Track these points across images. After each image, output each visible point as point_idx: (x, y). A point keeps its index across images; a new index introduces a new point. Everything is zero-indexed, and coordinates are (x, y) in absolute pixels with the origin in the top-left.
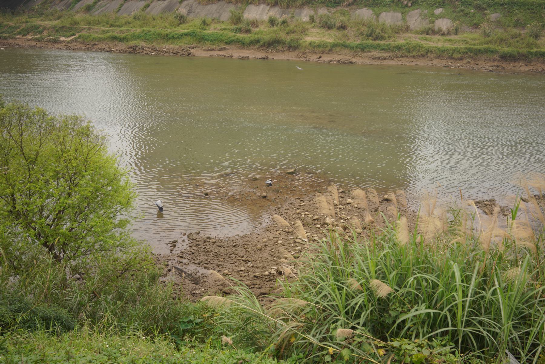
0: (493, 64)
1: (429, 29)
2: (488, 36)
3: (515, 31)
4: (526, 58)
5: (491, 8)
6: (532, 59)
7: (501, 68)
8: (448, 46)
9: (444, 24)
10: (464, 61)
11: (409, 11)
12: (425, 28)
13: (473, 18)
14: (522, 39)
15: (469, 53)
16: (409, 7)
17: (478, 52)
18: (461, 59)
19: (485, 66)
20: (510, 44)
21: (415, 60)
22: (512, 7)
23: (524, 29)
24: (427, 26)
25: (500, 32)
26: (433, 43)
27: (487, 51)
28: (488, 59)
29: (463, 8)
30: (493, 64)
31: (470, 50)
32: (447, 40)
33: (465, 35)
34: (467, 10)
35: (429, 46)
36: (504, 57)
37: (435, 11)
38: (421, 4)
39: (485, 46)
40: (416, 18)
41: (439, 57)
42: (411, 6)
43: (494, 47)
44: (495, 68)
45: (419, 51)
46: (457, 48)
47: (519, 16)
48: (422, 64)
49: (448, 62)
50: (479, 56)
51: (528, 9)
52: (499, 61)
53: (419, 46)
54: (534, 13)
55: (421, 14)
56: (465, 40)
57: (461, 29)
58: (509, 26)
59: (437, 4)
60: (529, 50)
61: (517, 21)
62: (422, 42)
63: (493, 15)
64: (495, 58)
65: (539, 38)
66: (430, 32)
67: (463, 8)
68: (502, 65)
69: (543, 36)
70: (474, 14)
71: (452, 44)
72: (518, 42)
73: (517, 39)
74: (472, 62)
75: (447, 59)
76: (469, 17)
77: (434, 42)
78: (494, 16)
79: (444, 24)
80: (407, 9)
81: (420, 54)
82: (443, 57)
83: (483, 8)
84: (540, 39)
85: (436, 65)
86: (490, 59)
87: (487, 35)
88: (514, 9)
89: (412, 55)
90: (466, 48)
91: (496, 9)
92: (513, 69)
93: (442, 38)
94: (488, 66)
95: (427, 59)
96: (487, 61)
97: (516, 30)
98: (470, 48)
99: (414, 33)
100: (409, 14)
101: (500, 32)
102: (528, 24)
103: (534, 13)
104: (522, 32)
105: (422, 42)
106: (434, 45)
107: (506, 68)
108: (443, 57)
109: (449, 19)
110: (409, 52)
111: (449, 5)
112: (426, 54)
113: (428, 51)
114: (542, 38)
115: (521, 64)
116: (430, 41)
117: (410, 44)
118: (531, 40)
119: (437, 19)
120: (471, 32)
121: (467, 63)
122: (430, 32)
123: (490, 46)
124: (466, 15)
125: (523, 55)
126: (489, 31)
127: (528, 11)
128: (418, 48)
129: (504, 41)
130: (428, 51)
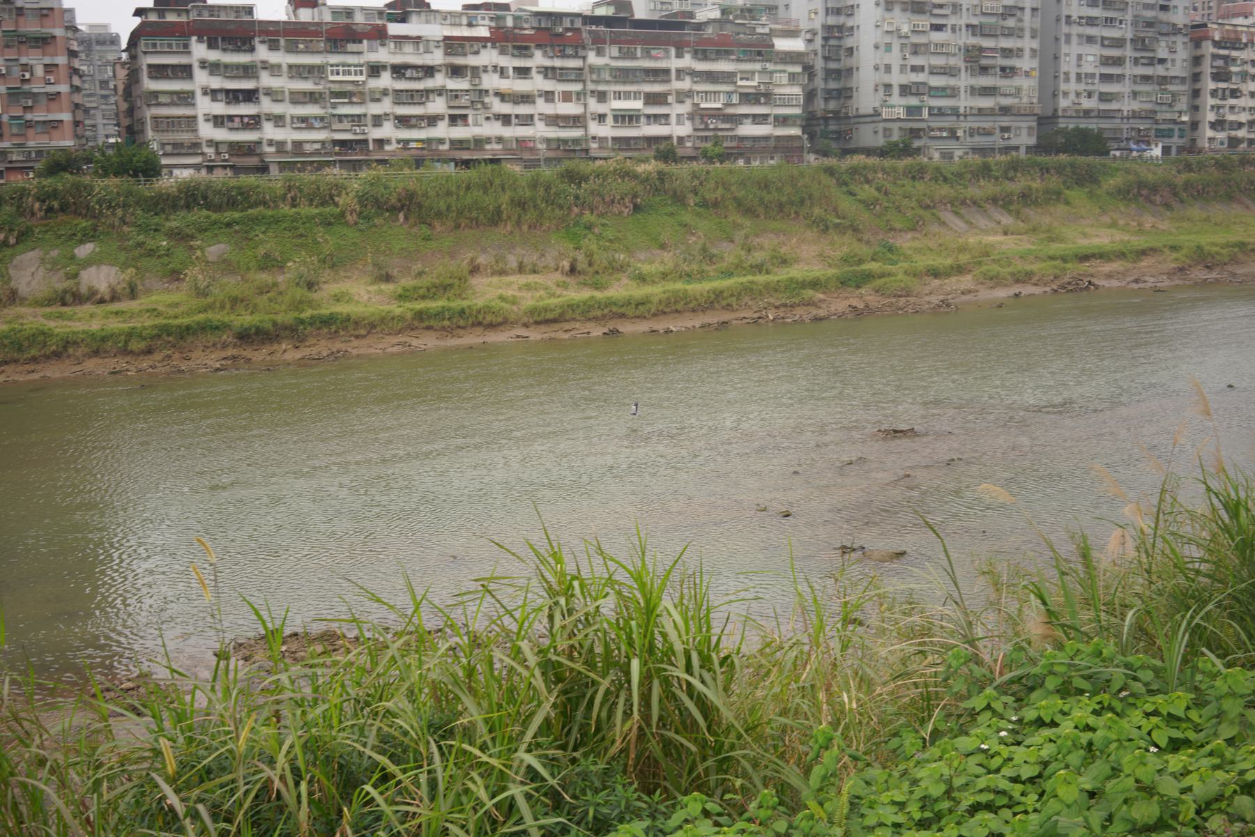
0: (224, 354)
1: (65, 292)
2: (202, 293)
3: (265, 277)
4: (294, 332)
5: (206, 234)
6: (306, 332)
7: (242, 361)
8: (115, 325)
9: (101, 278)
10: (158, 356)
11: (13, 256)
12: (56, 291)
13: (166, 260)
14: (281, 293)
15: (164, 335)
16: (13, 246)
17: (185, 332)
18: (149, 351)
19: (205, 359)
20: (255, 306)
21: (39, 367)
22: (252, 228)
23: (284, 273)
24: (60, 286)
25: (231, 285)
26: (78, 324)
27: (204, 328)
28: (210, 344)
29: (141, 238)
30: (224, 354)
31: (166, 330)
32: (112, 313)
33: (154, 298)
34: (151, 243)
35: (69, 330)
36: (246, 337)
37: (76, 251)
38: (40, 236)
39: (201, 317)
40: (33, 269)
41: (96, 353)
42: (17, 243)
43: (218, 317)
44: (229, 362)
45: (45, 344)
46: (134, 328)
47: (268, 246)
48: (57, 375)
49: (120, 363)
50: (189, 341)
51: (285, 229)
52: (235, 346)
53: (44, 334)
54: (301, 236)
55: (43, 261)
56: (155, 310)
57: (143, 285)
58: (248, 269)
59: (79, 235)
60: (296, 314)
61: (266, 256)
62: (52, 324)
63: (213, 249)
64: (226, 341)
65: (316, 287)
66: (69, 298)
67: (141, 238)
68: (244, 353)
69: (325, 282)
70: (169, 250)
71: (124, 321)
72: (270, 300)
73: (269, 295)
74: (177, 355)
75: (115, 356)
76: (159, 257)
77: (80, 320)
78: (215, 250)
79: (101, 278)
80: (8, 252)
81: (48, 351)
82: (106, 352)
83: (188, 236)
84: (320, 288)
85: (90, 373)
86: (214, 345)
87: (202, 293)
88: (257, 232)
89: (29, 356)
90: (155, 326)
91: (217, 235)
92: (268, 358)
93: (100, 310)
94: (213, 360)
95: (67, 362)
96: (208, 350)
97: (264, 276)
98: (165, 325)
99: (30, 305)
100: (15, 262)
101: (231, 285)
102: (289, 260)
103: (301, 236)
104: (280, 279)
105: (52, 324)
106: (81, 328)
107: (254, 359)
108: (106, 352)
109: (113, 265)
110: (20, 349)
111: (108, 233)
112: (63, 349)
113: (68, 343)
114: (325, 286)
115: (284, 346)
116: (69, 319)
117: (20, 331)
118: (300, 292)
119: (84, 268)
120: (168, 291)
121: (163, 360)
122: (69, 298)
123: (210, 315)
124: (151, 253)
125: (285, 328)
126: (205, 283)
127: (288, 234)
128: (41, 338)
129: (242, 301)
130: (68, 342)
